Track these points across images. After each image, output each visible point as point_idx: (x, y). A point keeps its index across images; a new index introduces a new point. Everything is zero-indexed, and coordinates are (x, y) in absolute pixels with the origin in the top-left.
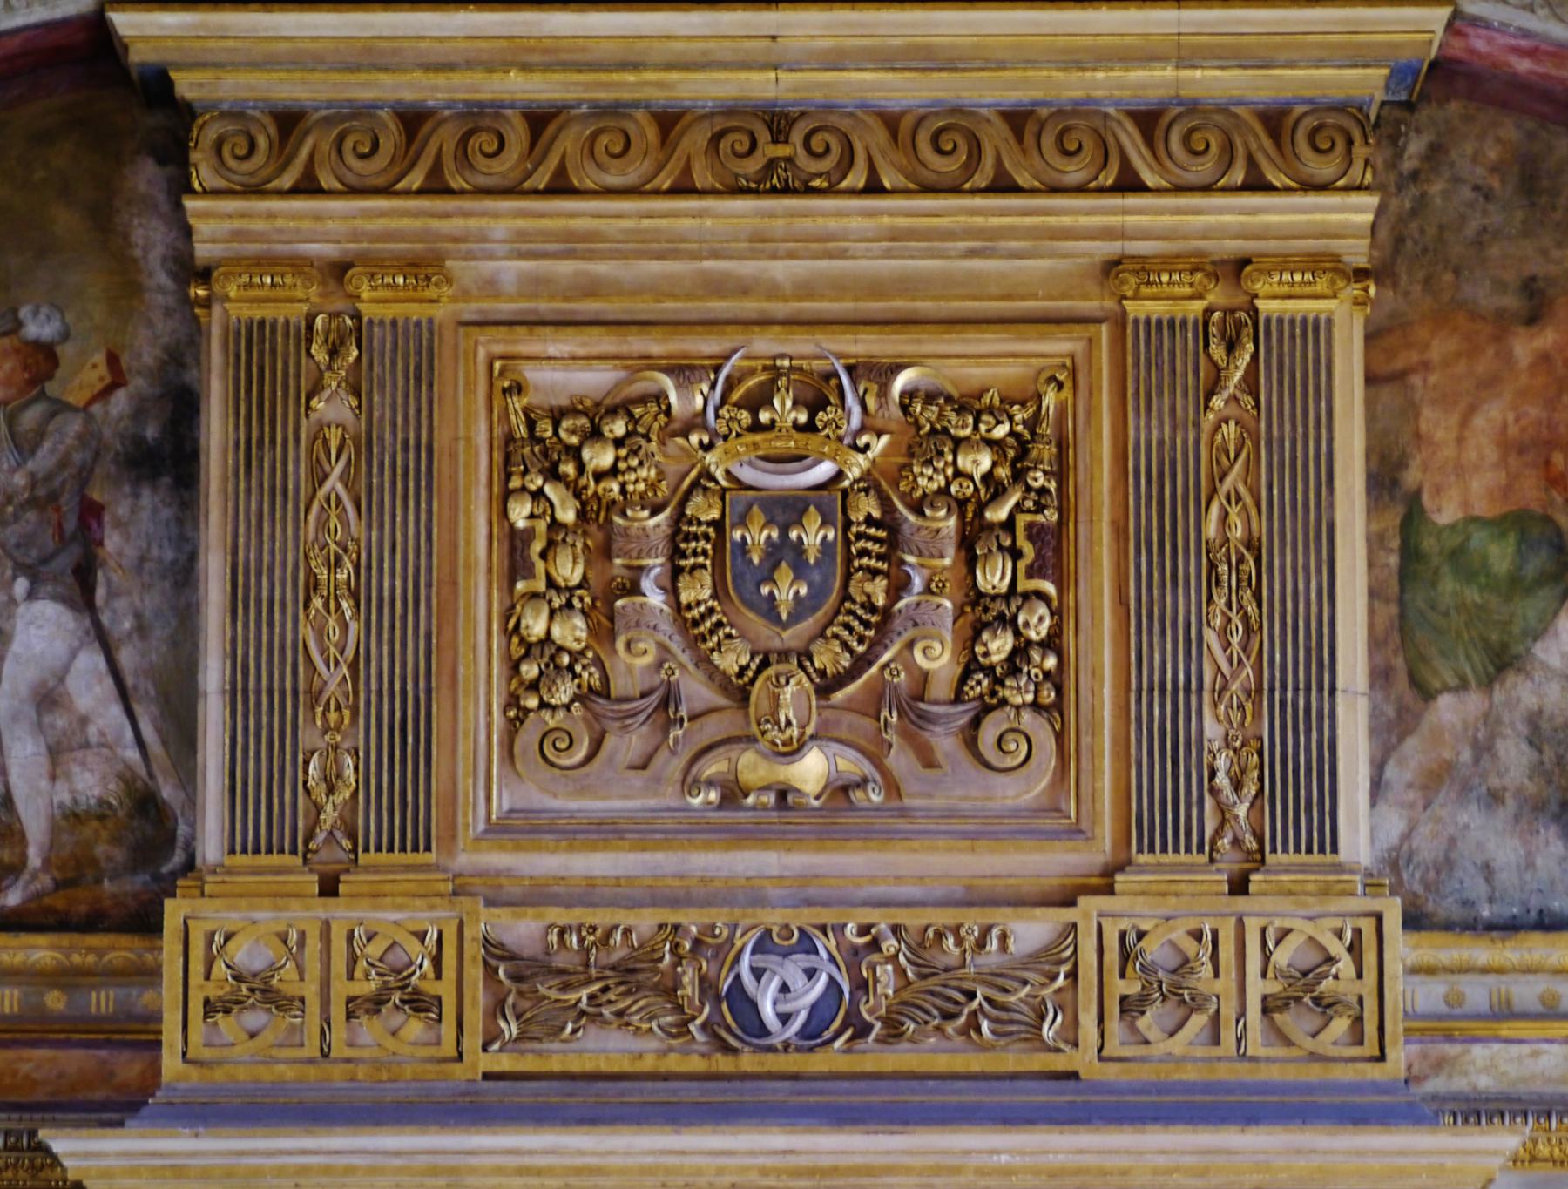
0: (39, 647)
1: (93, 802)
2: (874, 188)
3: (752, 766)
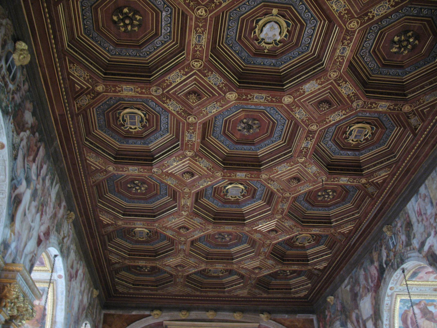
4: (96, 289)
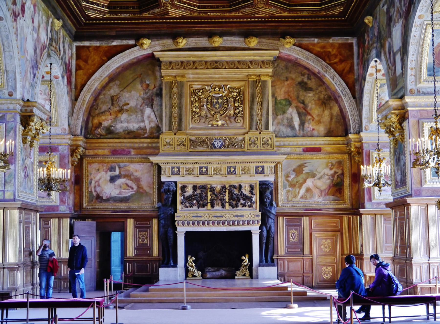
0: (148, 112)
2: (225, 68)
3: (214, 123)
4: (58, 19)
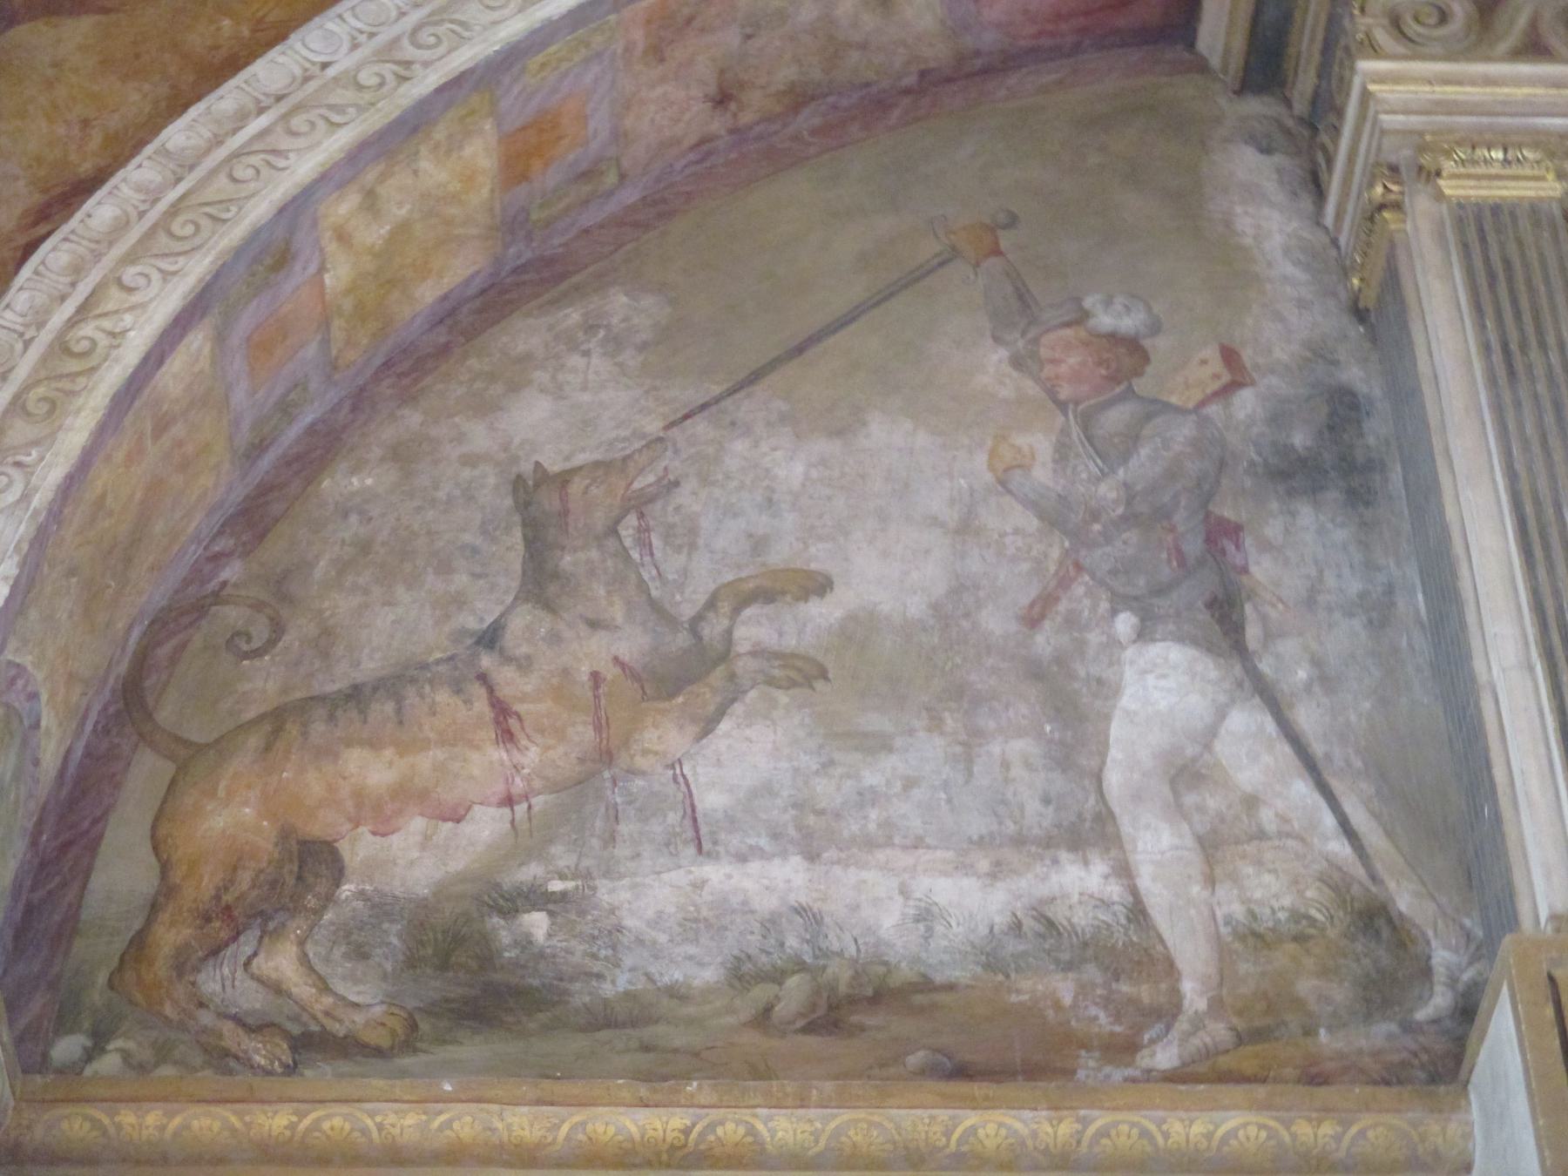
1: (1282, 916)
